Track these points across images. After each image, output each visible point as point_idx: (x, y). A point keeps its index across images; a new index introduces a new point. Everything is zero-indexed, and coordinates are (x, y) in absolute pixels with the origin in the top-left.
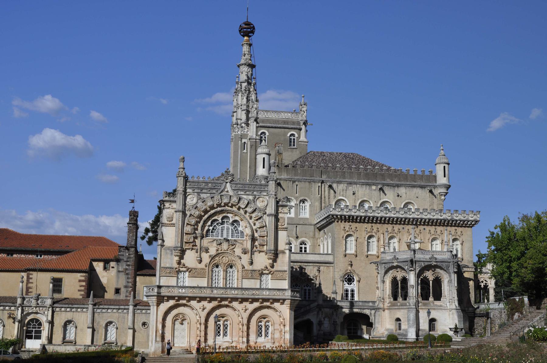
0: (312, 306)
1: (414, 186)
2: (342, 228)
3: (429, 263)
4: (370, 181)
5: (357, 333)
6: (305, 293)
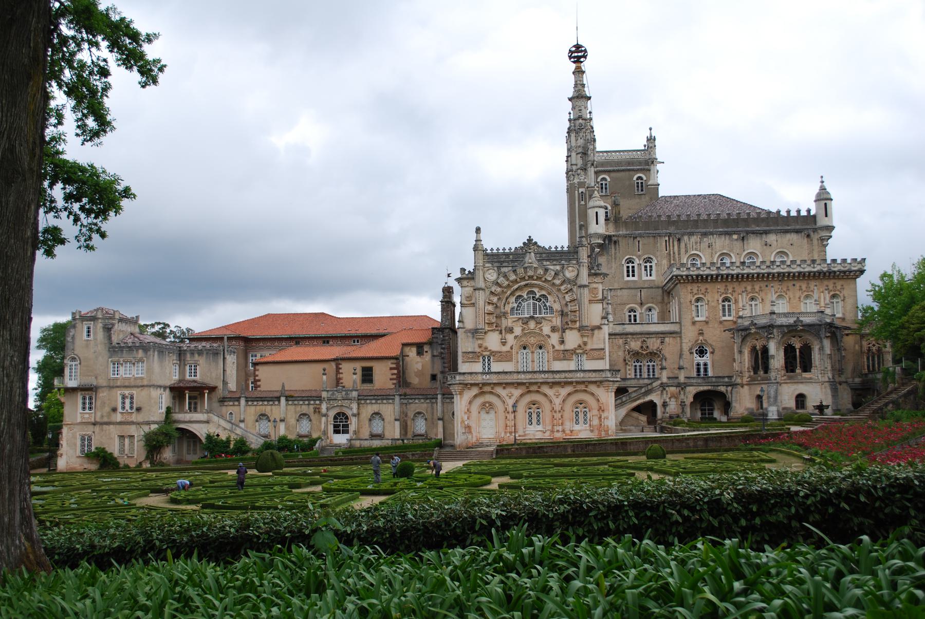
0: (655, 384)
1: (787, 232)
4: (730, 229)
5: (712, 414)
6: (649, 369)
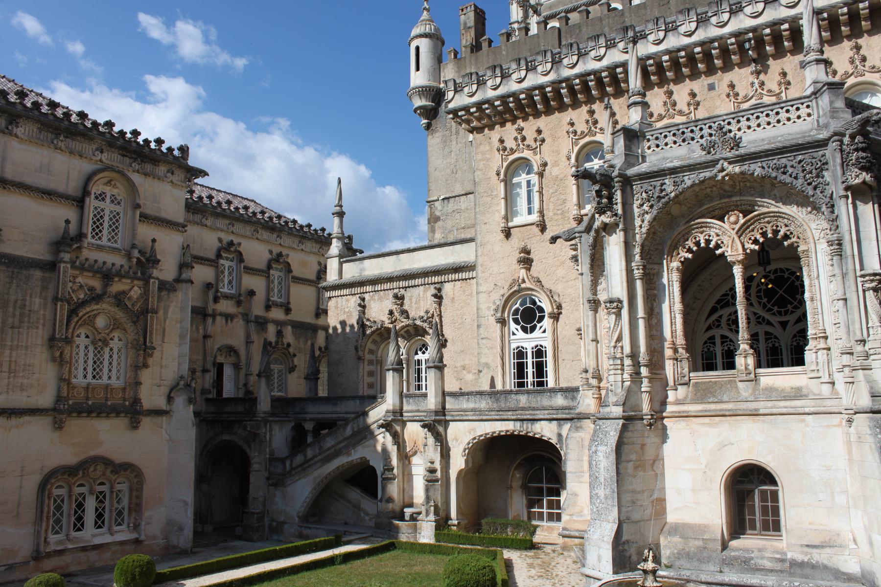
2: (496, 144)
3: (707, 174)
